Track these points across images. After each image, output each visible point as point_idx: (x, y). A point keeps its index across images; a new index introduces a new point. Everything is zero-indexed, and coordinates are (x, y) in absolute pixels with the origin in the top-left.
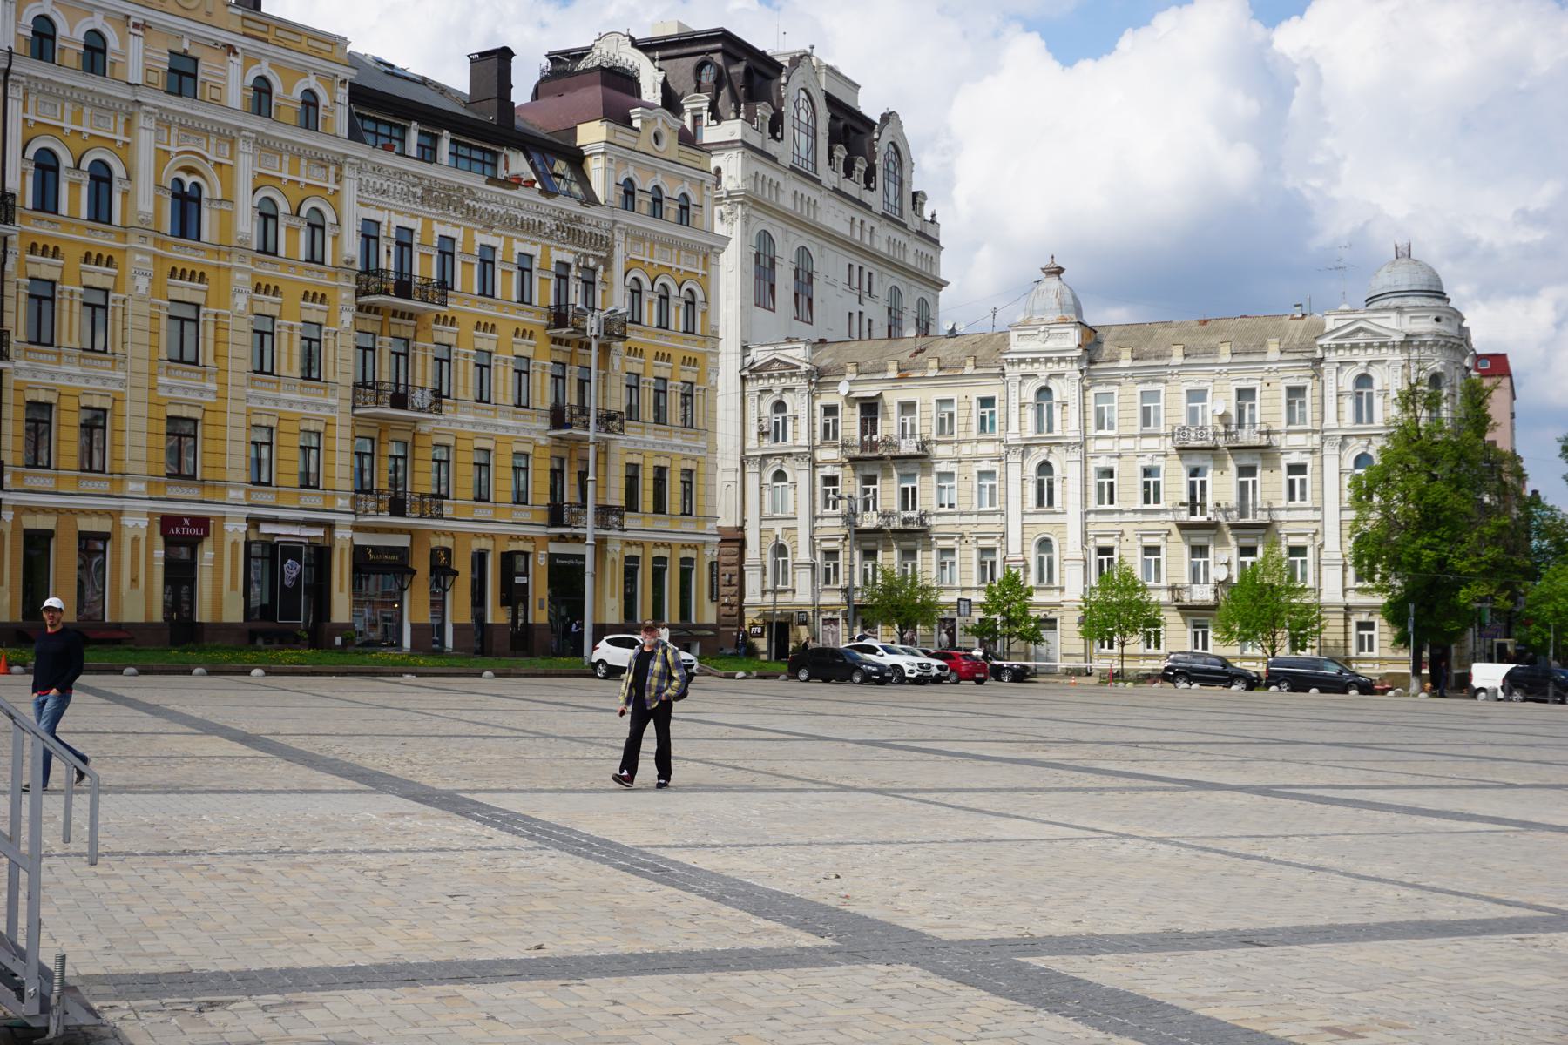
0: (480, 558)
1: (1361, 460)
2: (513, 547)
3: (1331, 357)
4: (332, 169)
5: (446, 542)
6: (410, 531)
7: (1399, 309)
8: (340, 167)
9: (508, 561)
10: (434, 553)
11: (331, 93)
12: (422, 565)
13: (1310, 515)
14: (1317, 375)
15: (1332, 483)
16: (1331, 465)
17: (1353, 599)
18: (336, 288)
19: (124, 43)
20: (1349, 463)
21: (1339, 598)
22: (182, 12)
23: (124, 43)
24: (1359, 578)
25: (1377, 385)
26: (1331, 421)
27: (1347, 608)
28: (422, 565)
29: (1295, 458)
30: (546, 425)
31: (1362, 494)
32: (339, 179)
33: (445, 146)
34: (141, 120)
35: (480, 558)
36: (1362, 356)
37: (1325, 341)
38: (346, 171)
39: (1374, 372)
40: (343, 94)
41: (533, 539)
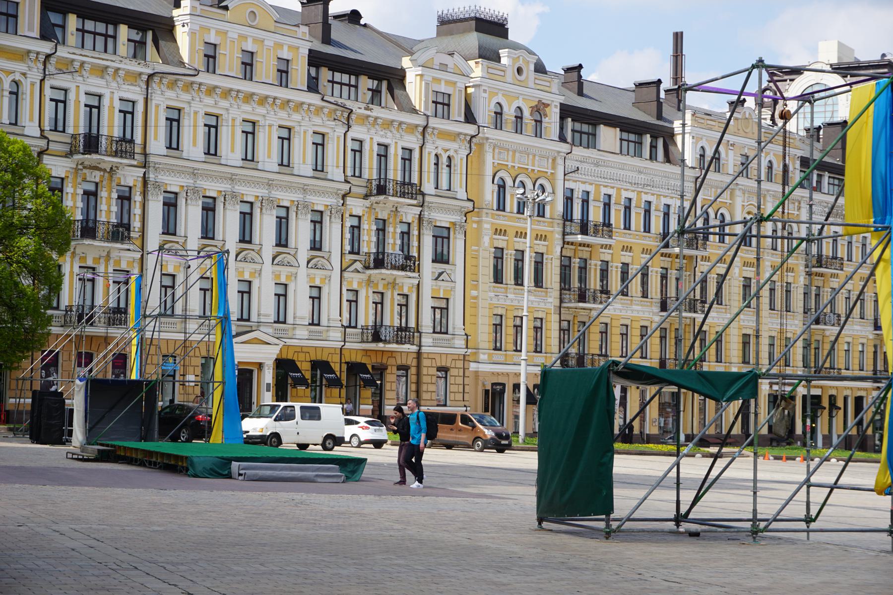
0: (846, 399)
2: (859, 394)
4: (797, 204)
5: (834, 392)
6: (821, 387)
8: (800, 203)
9: (859, 401)
10: (831, 396)
11: (794, 164)
12: (825, 403)
18: (797, 264)
19: (727, 155)
22: (744, 134)
23: (727, 155)
28: (825, 403)
30: (872, 328)
32: (799, 209)
33: (826, 180)
34: (738, 193)
35: (846, 399)
38: (803, 205)
40: (798, 163)
41: (866, 389)
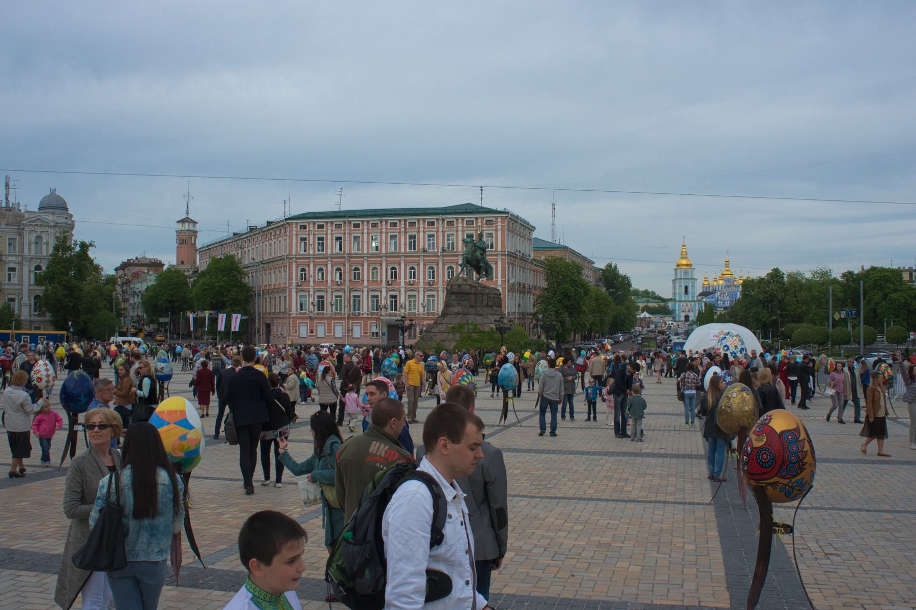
1: (38, 268)
3: (27, 228)
7: (53, 213)
13: (17, 287)
14: (20, 235)
15: (27, 276)
16: (26, 269)
17: (33, 318)
20: (33, 269)
21: (28, 318)
24: (35, 311)
25: (44, 240)
26: (26, 252)
27: (31, 321)
29: (12, 265)
31: (39, 281)
36: (39, 230)
37: (25, 222)
39: (43, 235)
